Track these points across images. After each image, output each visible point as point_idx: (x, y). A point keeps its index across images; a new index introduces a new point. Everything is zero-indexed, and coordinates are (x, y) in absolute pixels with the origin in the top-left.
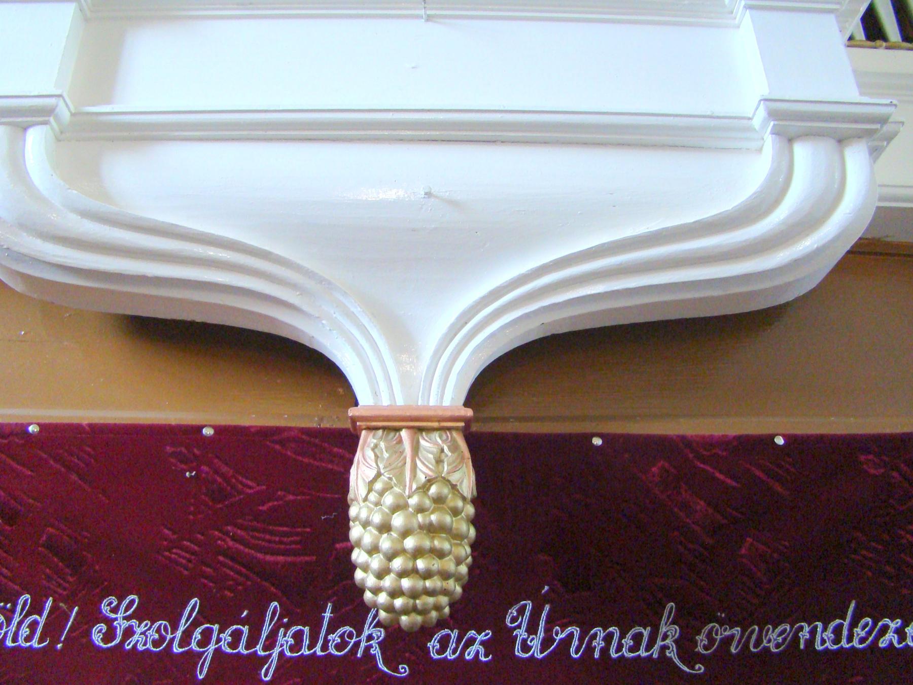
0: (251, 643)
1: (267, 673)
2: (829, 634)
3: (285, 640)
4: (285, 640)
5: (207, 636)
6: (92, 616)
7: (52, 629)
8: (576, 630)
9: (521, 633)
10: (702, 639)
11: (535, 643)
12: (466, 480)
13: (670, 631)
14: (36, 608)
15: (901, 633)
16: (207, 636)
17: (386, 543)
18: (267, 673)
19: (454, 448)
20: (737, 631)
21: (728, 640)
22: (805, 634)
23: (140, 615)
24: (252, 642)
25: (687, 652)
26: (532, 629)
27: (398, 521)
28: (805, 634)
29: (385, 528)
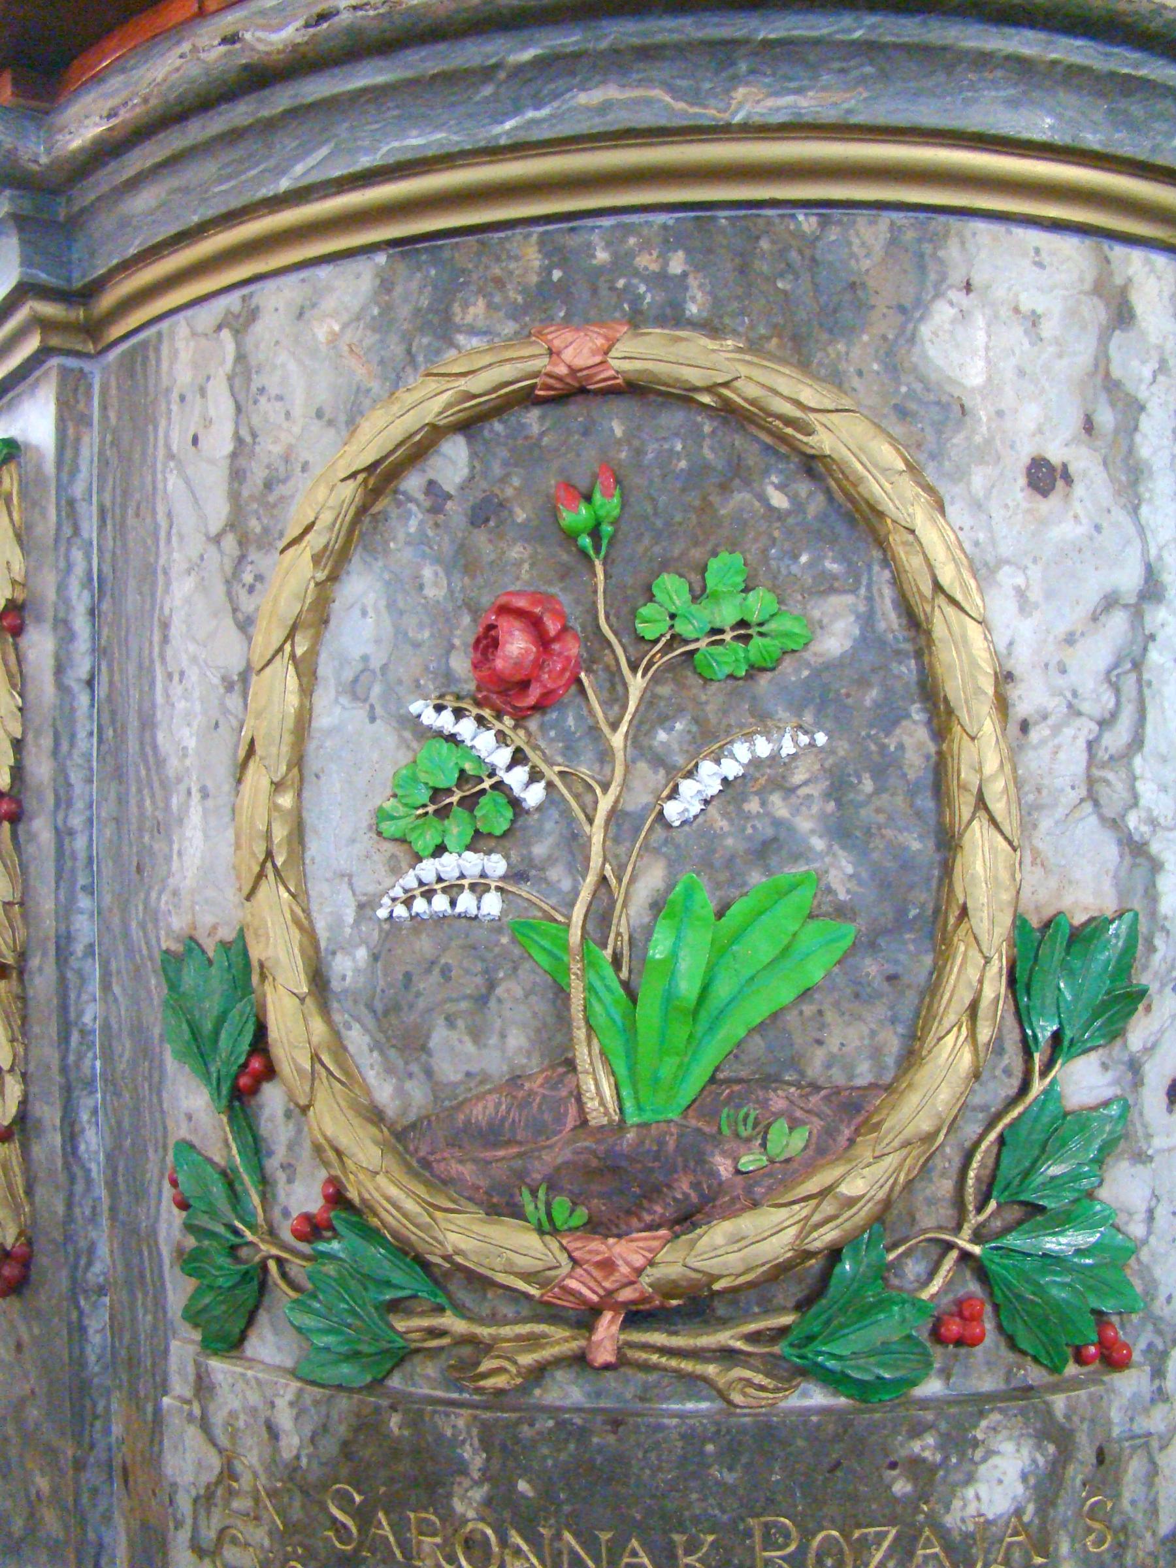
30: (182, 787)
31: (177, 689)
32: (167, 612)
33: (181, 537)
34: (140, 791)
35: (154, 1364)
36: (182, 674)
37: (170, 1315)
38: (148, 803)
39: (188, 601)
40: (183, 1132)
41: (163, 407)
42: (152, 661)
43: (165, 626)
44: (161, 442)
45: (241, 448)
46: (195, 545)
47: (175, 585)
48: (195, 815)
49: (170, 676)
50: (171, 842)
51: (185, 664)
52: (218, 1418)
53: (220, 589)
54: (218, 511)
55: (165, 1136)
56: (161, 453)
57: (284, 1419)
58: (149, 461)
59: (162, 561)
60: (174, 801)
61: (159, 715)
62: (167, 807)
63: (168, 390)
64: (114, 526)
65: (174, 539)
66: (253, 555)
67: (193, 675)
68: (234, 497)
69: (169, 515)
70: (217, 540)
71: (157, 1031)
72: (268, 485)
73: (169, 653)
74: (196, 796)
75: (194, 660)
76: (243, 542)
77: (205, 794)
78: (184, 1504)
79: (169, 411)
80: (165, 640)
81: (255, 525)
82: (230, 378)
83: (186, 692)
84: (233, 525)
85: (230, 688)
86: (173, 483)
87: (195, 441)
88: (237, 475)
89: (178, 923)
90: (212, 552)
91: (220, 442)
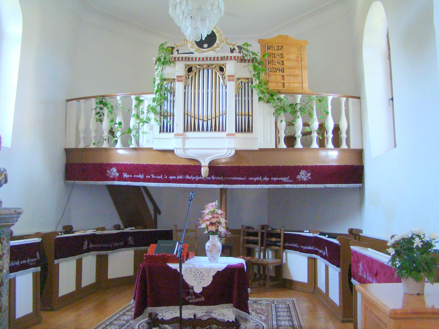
0: (196, 178)
1: (197, 180)
2: (234, 178)
3: (198, 178)
4: (198, 178)
5: (193, 178)
6: (185, 176)
7: (183, 177)
8: (216, 178)
9: (213, 178)
10: (224, 178)
11: (213, 178)
12: (208, 170)
13: (222, 178)
14: (182, 176)
15: (239, 179)
16: (193, 178)
17: (203, 174)
18: (197, 180)
19: (207, 168)
20: (227, 178)
21: (226, 179)
22: (232, 178)
23: (189, 176)
24: (196, 178)
25: (223, 179)
26: (213, 177)
27: (204, 172)
28: (232, 178)
29: (203, 173)
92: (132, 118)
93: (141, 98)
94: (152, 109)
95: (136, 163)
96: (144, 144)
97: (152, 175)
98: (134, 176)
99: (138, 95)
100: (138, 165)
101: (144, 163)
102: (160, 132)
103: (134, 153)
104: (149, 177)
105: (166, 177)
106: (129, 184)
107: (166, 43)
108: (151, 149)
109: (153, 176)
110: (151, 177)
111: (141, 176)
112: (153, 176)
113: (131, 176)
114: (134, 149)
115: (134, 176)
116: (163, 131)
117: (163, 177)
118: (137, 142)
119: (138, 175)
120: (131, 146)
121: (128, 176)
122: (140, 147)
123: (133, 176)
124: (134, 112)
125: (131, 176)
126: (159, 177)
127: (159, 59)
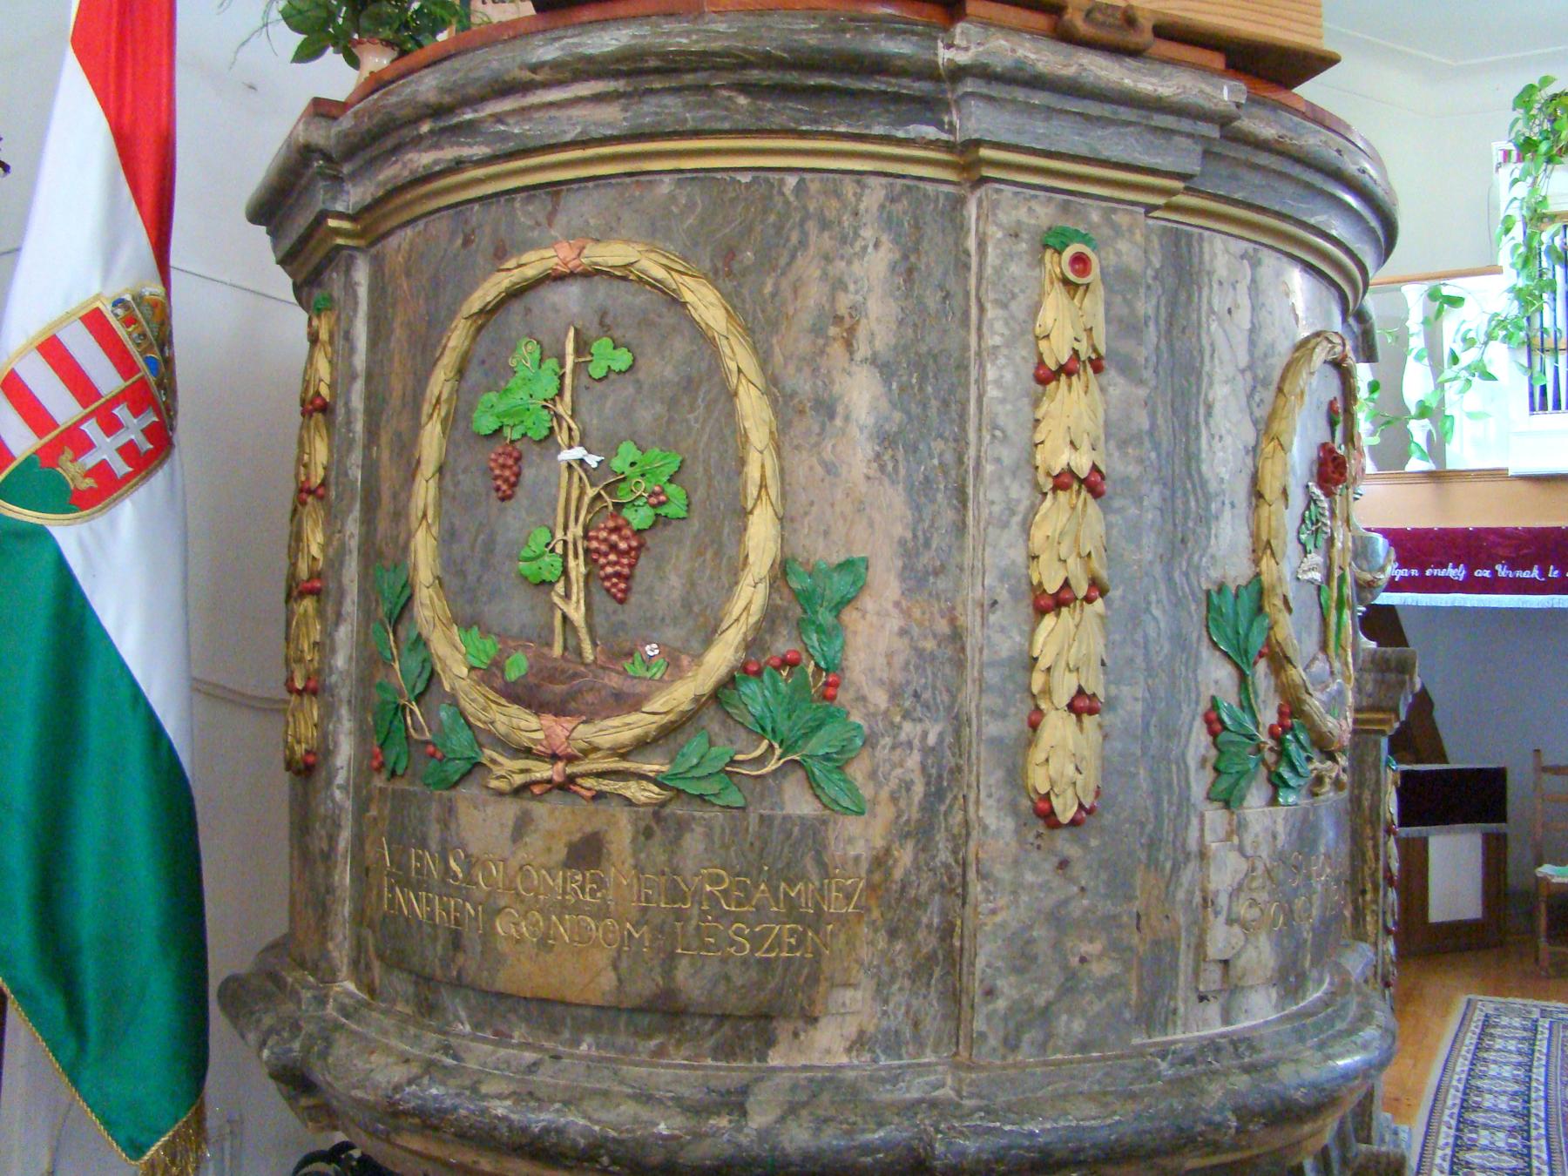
30: (1220, 499)
31: (1217, 445)
32: (1210, 397)
33: (1221, 362)
34: (1185, 494)
35: (1176, 836)
36: (1221, 438)
37: (1193, 800)
38: (1193, 504)
39: (1225, 398)
40: (1212, 692)
41: (1206, 279)
42: (1198, 423)
43: (1209, 407)
44: (1205, 300)
45: (1254, 330)
46: (1230, 370)
47: (1217, 386)
48: (1227, 514)
49: (1213, 436)
50: (1209, 529)
51: (1223, 432)
52: (1248, 840)
53: (1244, 400)
54: (1243, 359)
55: (1198, 695)
56: (1205, 307)
57: (1280, 829)
58: (1194, 305)
59: (1207, 368)
60: (1213, 506)
61: (1204, 456)
62: (1207, 509)
63: (1210, 274)
64: (1158, 331)
65: (1216, 361)
66: (1259, 388)
67: (1228, 440)
68: (1251, 353)
69: (1212, 345)
70: (1243, 372)
71: (1194, 637)
72: (1266, 355)
73: (1212, 422)
74: (1228, 506)
75: (1229, 432)
76: (1255, 378)
77: (1233, 506)
78: (1223, 900)
79: (1211, 287)
80: (1209, 414)
81: (1261, 374)
82: (1249, 289)
83: (1224, 449)
84: (1251, 367)
85: (1247, 453)
86: (1214, 326)
87: (1230, 311)
88: (1252, 343)
89: (1215, 574)
90: (1239, 377)
91: (1243, 317)
92: (1410, 360)
93: (1446, 291)
94: (1499, 327)
95: (1436, 524)
96: (1459, 456)
97: (1498, 567)
98: (1428, 573)
99: (1436, 282)
100: (1444, 532)
101: (1471, 524)
102: (1532, 409)
103: (1425, 490)
104: (1487, 573)
105: (1553, 573)
106: (1409, 602)
107: (1546, 81)
108: (1498, 474)
109: (1502, 571)
110: (1494, 572)
111: (1455, 572)
112: (1502, 571)
113: (1414, 572)
114: (1431, 476)
115: (1428, 573)
116: (1544, 407)
117: (1544, 572)
118: (1436, 448)
119: (1444, 566)
120: (1416, 464)
121: (1404, 572)
122: (1450, 466)
123: (1422, 572)
124: (1417, 343)
125: (1414, 572)
126: (1525, 574)
127: (1527, 147)
